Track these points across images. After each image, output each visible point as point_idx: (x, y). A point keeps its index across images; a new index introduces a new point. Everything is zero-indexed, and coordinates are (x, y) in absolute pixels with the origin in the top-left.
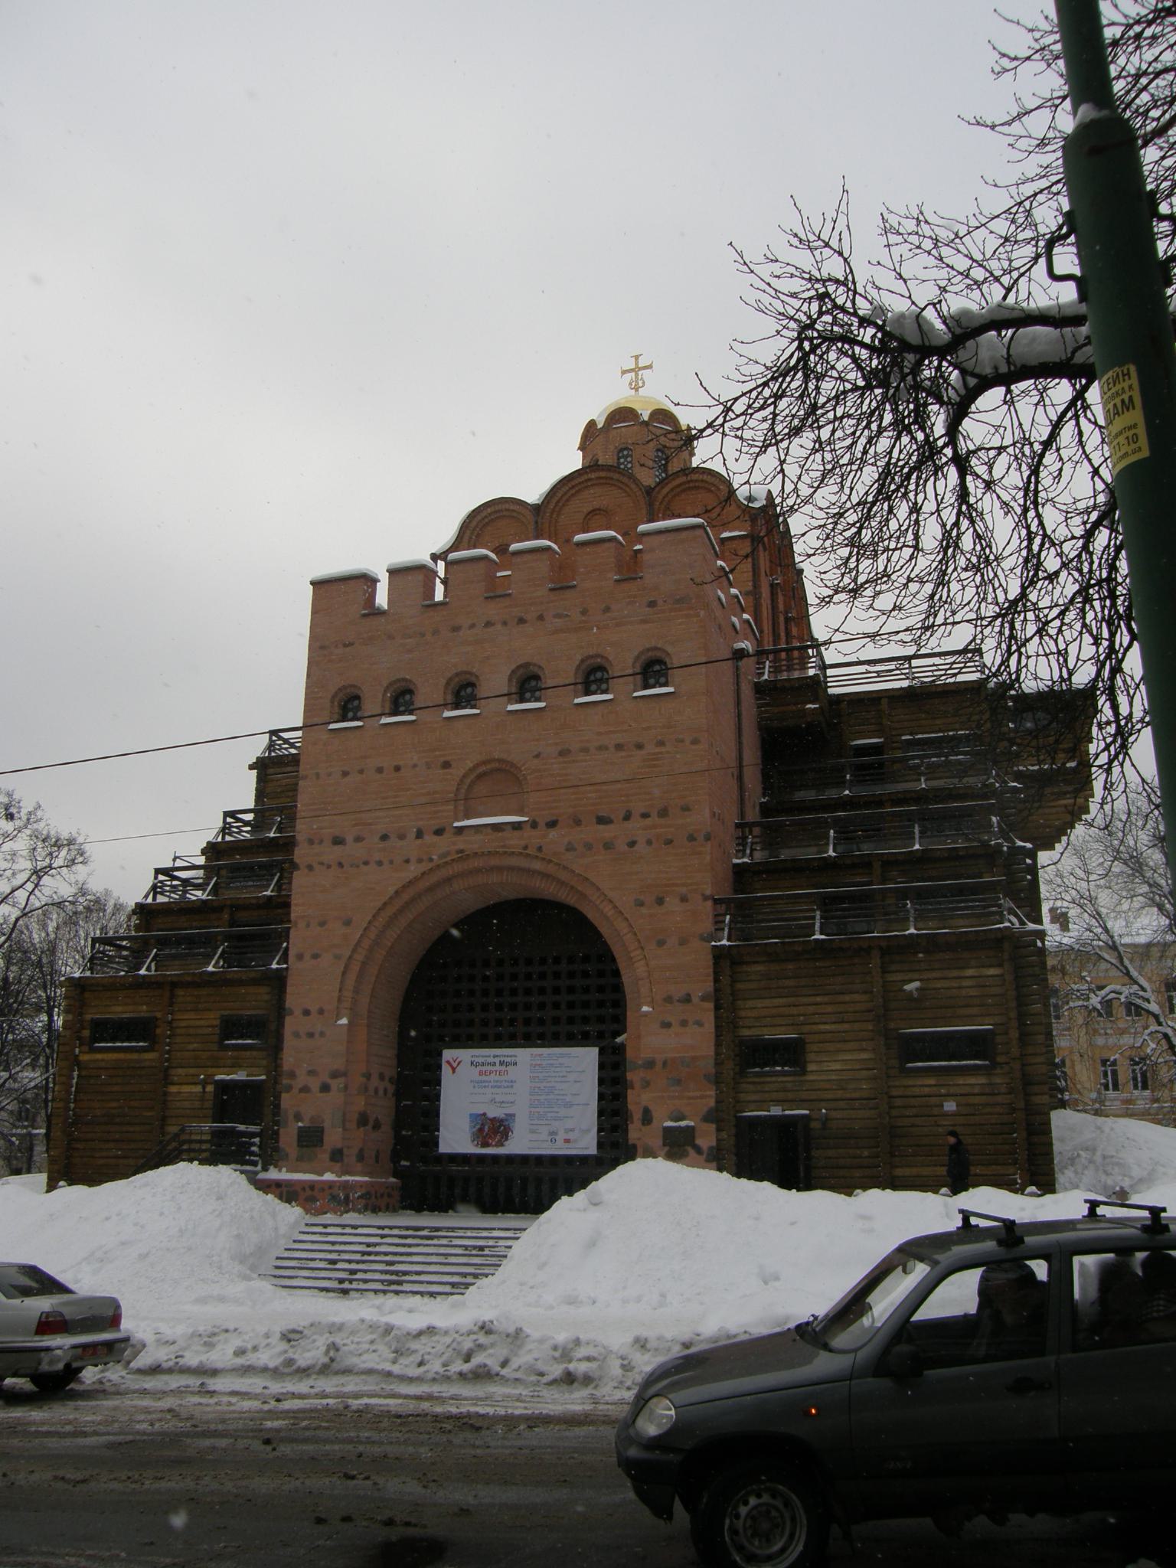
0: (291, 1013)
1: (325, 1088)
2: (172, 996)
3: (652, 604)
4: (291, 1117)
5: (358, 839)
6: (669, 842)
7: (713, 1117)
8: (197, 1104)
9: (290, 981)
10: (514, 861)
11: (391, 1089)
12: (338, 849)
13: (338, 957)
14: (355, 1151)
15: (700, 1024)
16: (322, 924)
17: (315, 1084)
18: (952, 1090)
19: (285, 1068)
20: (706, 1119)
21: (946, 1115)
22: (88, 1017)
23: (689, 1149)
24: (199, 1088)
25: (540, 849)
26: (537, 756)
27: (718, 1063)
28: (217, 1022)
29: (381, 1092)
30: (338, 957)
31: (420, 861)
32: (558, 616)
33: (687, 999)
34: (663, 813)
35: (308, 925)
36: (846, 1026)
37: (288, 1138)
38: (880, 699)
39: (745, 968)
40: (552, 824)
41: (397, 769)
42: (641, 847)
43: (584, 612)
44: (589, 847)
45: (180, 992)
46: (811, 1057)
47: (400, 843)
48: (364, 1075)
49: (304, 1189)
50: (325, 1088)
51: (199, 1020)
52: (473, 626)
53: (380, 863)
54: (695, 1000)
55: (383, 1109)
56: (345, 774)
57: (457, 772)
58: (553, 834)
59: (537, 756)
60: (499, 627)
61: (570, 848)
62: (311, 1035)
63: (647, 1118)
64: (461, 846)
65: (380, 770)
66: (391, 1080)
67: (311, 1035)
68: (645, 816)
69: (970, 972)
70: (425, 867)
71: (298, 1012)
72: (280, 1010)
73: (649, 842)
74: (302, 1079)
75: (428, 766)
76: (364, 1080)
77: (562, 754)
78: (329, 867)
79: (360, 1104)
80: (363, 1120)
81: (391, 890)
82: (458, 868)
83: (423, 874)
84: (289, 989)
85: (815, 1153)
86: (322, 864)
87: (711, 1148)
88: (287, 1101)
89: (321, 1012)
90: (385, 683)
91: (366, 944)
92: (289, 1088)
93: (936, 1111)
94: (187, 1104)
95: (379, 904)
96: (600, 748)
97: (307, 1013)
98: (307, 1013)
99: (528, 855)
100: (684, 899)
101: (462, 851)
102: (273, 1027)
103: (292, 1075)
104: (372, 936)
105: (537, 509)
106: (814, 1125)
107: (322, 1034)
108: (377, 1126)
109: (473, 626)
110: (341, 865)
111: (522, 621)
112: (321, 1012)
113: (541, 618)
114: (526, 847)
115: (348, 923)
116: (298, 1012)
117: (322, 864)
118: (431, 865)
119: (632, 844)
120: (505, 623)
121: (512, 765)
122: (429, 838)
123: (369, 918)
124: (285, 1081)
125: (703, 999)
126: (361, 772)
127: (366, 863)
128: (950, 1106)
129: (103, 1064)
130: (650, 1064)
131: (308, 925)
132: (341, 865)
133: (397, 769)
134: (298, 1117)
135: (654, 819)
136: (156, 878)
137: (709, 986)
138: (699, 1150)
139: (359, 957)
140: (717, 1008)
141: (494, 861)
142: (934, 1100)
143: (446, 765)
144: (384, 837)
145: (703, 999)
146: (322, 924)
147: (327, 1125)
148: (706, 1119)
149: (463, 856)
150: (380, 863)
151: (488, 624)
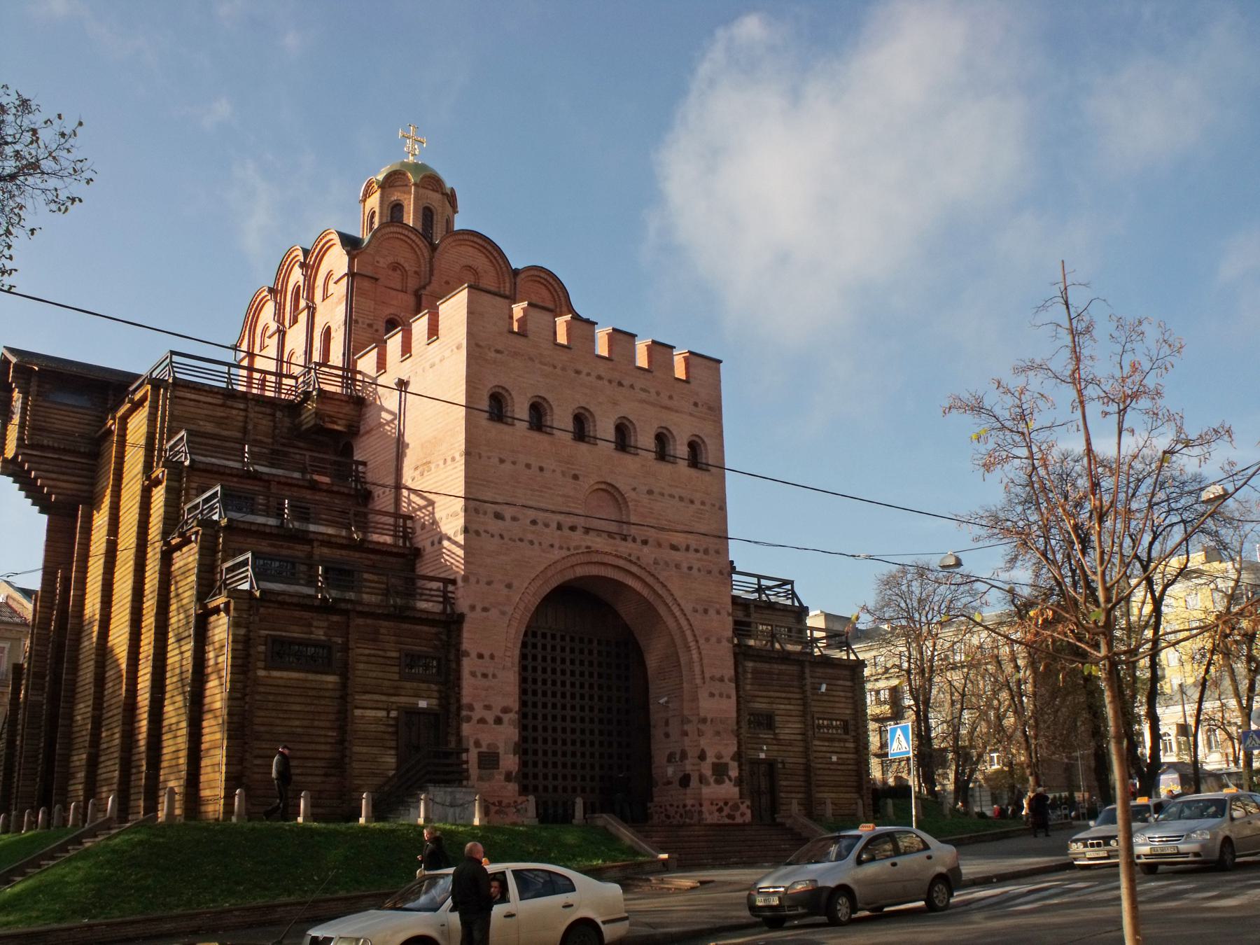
0: (467, 654)
1: (498, 721)
3: (696, 404)
5: (514, 519)
6: (709, 572)
7: (738, 756)
8: (382, 728)
10: (621, 563)
12: (500, 522)
13: (503, 613)
15: (729, 697)
16: (489, 583)
17: (490, 717)
19: (465, 700)
20: (733, 759)
21: (833, 763)
24: (384, 713)
25: (638, 558)
26: (634, 489)
27: (738, 722)
30: (503, 613)
31: (561, 548)
32: (642, 390)
33: (721, 680)
35: (478, 582)
40: (645, 542)
41: (541, 469)
42: (695, 571)
43: (658, 394)
44: (667, 564)
47: (546, 530)
50: (498, 721)
52: (588, 374)
53: (532, 543)
56: (502, 461)
58: (646, 549)
59: (634, 489)
61: (656, 563)
62: (485, 676)
63: (702, 756)
64: (589, 544)
65: (528, 466)
67: (485, 676)
68: (697, 551)
70: (564, 553)
71: (474, 655)
73: (699, 570)
74: (478, 713)
75: (563, 474)
78: (492, 536)
86: (486, 532)
88: (466, 729)
89: (492, 657)
90: (529, 396)
92: (469, 719)
95: (533, 576)
96: (672, 496)
97: (481, 656)
98: (481, 656)
99: (630, 561)
100: (718, 613)
103: (471, 708)
106: (780, 766)
107: (494, 676)
109: (588, 374)
110: (502, 537)
111: (620, 384)
112: (492, 657)
113: (632, 386)
115: (509, 586)
116: (474, 655)
117: (486, 532)
118: (568, 553)
119: (690, 568)
120: (610, 381)
121: (617, 489)
122: (567, 532)
123: (525, 585)
124: (464, 713)
125: (730, 680)
126: (514, 463)
127: (521, 540)
129: (281, 682)
130: (704, 721)
131: (478, 582)
132: (502, 537)
134: (477, 744)
137: (732, 672)
138: (730, 780)
143: (576, 477)
144: (534, 522)
146: (489, 583)
147: (501, 751)
148: (733, 759)
149: (589, 551)
150: (532, 543)
151: (599, 378)
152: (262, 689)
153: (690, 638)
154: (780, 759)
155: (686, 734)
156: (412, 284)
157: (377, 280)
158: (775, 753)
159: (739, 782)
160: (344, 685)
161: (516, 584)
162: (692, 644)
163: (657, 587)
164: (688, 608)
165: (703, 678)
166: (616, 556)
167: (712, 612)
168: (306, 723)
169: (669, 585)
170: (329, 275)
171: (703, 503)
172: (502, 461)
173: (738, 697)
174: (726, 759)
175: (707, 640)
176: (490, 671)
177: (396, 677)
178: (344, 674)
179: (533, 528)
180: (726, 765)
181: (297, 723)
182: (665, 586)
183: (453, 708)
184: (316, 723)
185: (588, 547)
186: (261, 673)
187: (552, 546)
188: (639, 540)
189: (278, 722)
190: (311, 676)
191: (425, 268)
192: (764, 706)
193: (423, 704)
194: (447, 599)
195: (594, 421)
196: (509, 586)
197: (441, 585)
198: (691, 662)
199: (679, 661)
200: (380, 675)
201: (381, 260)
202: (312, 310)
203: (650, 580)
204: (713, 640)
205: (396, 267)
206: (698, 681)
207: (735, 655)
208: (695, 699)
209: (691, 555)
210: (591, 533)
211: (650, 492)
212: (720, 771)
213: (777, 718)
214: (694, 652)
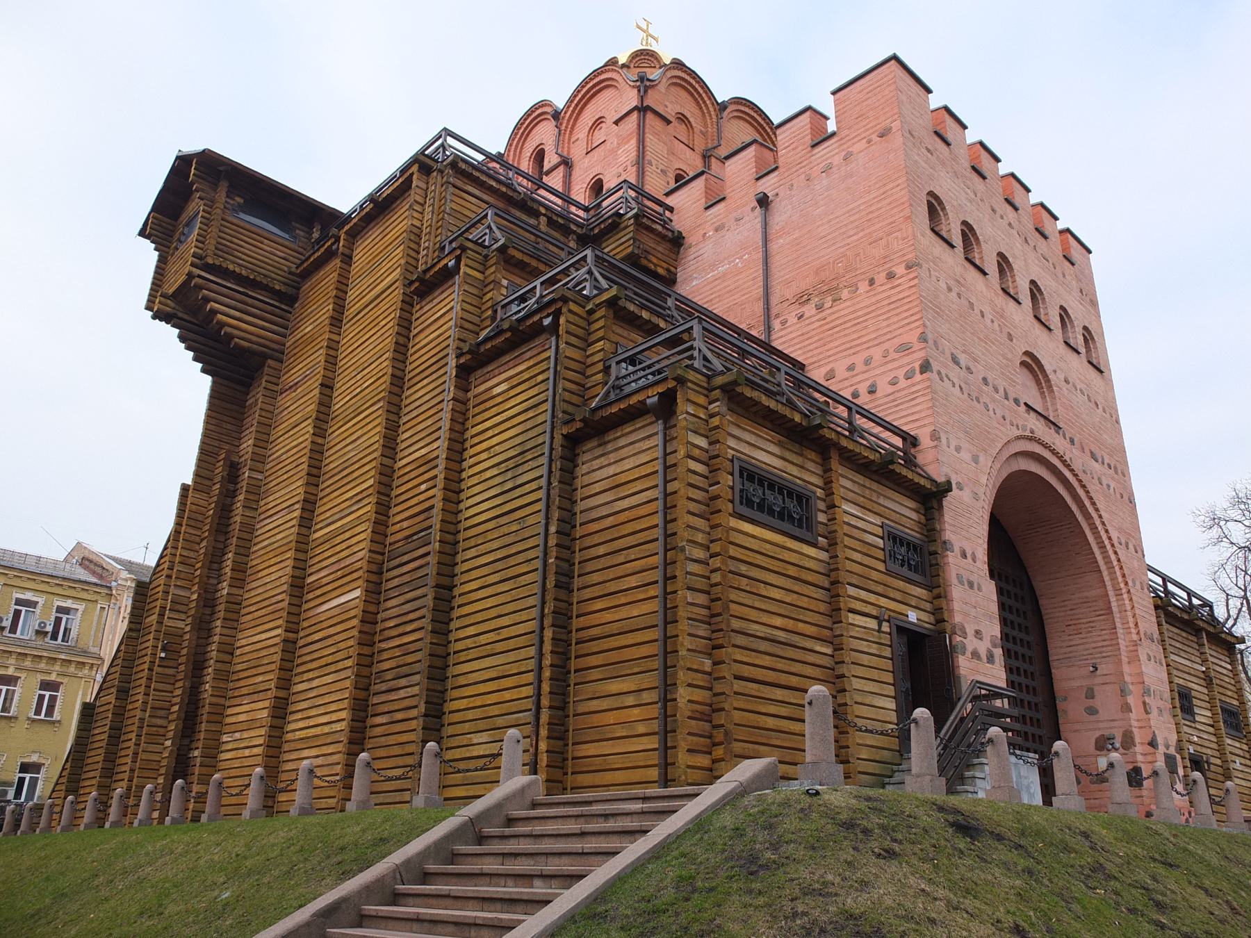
7: (1180, 749)
8: (874, 649)
17: (983, 647)
19: (958, 619)
24: (873, 624)
30: (976, 497)
34: (1116, 472)
46: (1196, 710)
50: (991, 658)
56: (950, 290)
62: (971, 585)
63: (1153, 744)
67: (971, 585)
69: (1223, 664)
71: (957, 549)
74: (971, 643)
81: (1000, 446)
94: (863, 646)
98: (964, 555)
107: (979, 589)
115: (976, 460)
118: (1019, 433)
123: (990, 464)
129: (754, 544)
135: (1112, 471)
143: (1010, 337)
146: (958, 449)
152: (733, 551)
153: (1120, 579)
155: (1127, 708)
156: (700, 145)
157: (669, 122)
160: (832, 570)
161: (982, 459)
162: (1122, 585)
163: (1087, 503)
164: (1114, 535)
165: (1138, 633)
166: (1054, 452)
167: (1131, 546)
169: (1099, 505)
170: (599, 122)
171: (1104, 411)
172: (950, 290)
173: (1168, 665)
174: (1172, 751)
175: (1134, 581)
176: (974, 578)
178: (833, 543)
179: (984, 388)
180: (1175, 758)
181: (778, 621)
182: (1093, 504)
183: (948, 628)
185: (1032, 432)
186: (734, 523)
187: (1004, 418)
189: (754, 615)
191: (712, 130)
192: (1181, 682)
193: (913, 616)
194: (910, 462)
195: (1013, 276)
196: (976, 460)
197: (898, 442)
198: (1123, 611)
199: (1110, 608)
200: (867, 560)
201: (670, 106)
202: (566, 163)
203: (1081, 492)
204: (1138, 586)
205: (682, 118)
206: (1135, 637)
207: (1156, 607)
208: (1134, 659)
209: (1105, 469)
210: (1032, 414)
211: (1067, 381)
213: (1195, 702)
214: (1125, 596)
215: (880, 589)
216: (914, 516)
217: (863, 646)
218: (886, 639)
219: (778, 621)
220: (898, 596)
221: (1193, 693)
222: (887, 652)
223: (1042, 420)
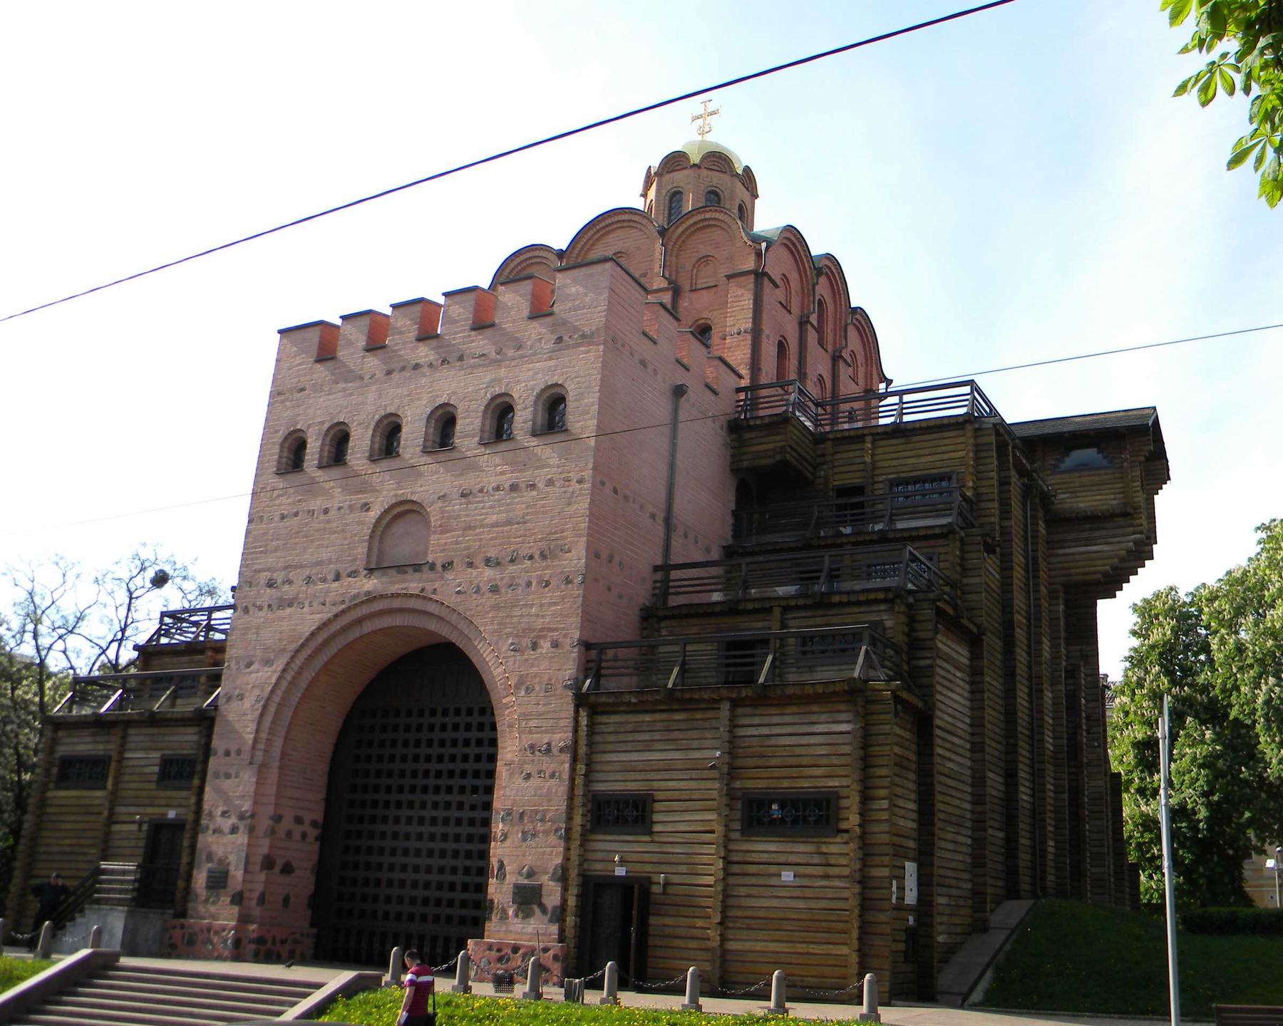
1: (234, 830)
2: (124, 738)
4: (204, 857)
8: (133, 843)
9: (217, 723)
10: (411, 603)
11: (313, 833)
14: (256, 895)
17: (227, 824)
18: (792, 859)
22: (58, 755)
23: (535, 907)
28: (158, 761)
29: (297, 836)
36: (693, 784)
37: (200, 879)
38: (864, 435)
39: (604, 719)
45: (132, 731)
46: (656, 817)
48: (272, 818)
49: (202, 931)
50: (234, 830)
51: (144, 757)
54: (555, 750)
55: (305, 855)
57: (374, 514)
60: (426, 369)
63: (502, 875)
66: (314, 824)
69: (820, 728)
71: (221, 752)
72: (207, 751)
76: (270, 822)
77: (463, 495)
79: (264, 847)
80: (268, 863)
82: (365, 610)
83: (336, 616)
84: (217, 729)
85: (653, 920)
87: (555, 908)
89: (239, 752)
91: (284, 684)
93: (773, 881)
94: (125, 843)
100: (555, 645)
101: (369, 593)
102: (199, 768)
104: (289, 678)
105: (561, 254)
106: (656, 889)
108: (287, 869)
112: (239, 752)
114: (423, 590)
116: (221, 752)
128: (787, 876)
133: (326, 511)
136: (161, 622)
138: (544, 911)
139: (277, 699)
140: (575, 760)
141: (396, 604)
142: (773, 869)
145: (561, 750)
149: (371, 598)
154: (655, 878)
158: (648, 868)
159: (559, 915)
167: (545, 645)
168: (75, 841)
177: (153, 786)
184: (82, 841)
188: (439, 568)
190: (85, 793)
193: (172, 814)
212: (527, 898)
215: (147, 801)
216: (195, 738)
217: (125, 843)
218: (143, 835)
219: (68, 842)
220: (163, 802)
221: (659, 795)
222: (142, 843)
223: (393, 572)
